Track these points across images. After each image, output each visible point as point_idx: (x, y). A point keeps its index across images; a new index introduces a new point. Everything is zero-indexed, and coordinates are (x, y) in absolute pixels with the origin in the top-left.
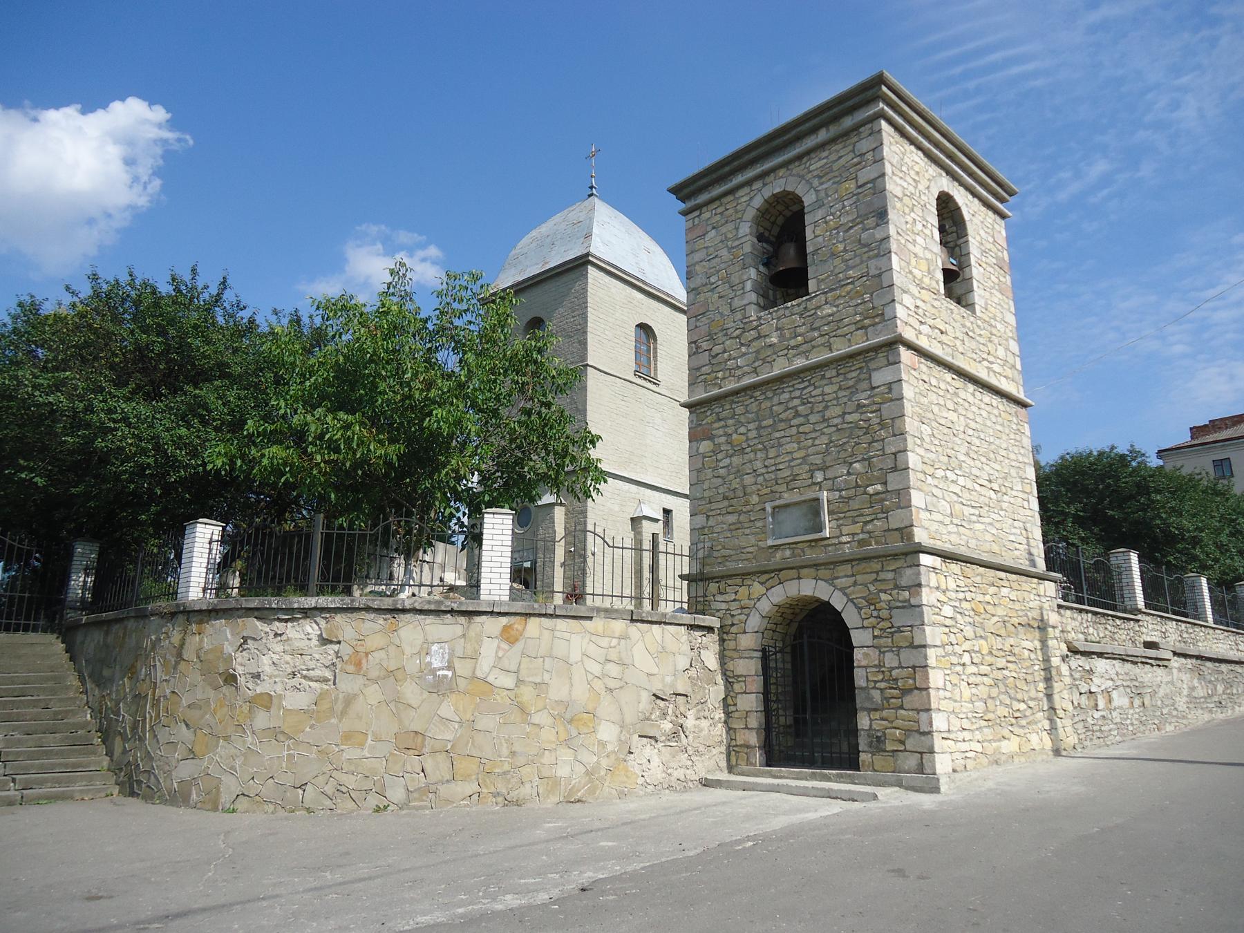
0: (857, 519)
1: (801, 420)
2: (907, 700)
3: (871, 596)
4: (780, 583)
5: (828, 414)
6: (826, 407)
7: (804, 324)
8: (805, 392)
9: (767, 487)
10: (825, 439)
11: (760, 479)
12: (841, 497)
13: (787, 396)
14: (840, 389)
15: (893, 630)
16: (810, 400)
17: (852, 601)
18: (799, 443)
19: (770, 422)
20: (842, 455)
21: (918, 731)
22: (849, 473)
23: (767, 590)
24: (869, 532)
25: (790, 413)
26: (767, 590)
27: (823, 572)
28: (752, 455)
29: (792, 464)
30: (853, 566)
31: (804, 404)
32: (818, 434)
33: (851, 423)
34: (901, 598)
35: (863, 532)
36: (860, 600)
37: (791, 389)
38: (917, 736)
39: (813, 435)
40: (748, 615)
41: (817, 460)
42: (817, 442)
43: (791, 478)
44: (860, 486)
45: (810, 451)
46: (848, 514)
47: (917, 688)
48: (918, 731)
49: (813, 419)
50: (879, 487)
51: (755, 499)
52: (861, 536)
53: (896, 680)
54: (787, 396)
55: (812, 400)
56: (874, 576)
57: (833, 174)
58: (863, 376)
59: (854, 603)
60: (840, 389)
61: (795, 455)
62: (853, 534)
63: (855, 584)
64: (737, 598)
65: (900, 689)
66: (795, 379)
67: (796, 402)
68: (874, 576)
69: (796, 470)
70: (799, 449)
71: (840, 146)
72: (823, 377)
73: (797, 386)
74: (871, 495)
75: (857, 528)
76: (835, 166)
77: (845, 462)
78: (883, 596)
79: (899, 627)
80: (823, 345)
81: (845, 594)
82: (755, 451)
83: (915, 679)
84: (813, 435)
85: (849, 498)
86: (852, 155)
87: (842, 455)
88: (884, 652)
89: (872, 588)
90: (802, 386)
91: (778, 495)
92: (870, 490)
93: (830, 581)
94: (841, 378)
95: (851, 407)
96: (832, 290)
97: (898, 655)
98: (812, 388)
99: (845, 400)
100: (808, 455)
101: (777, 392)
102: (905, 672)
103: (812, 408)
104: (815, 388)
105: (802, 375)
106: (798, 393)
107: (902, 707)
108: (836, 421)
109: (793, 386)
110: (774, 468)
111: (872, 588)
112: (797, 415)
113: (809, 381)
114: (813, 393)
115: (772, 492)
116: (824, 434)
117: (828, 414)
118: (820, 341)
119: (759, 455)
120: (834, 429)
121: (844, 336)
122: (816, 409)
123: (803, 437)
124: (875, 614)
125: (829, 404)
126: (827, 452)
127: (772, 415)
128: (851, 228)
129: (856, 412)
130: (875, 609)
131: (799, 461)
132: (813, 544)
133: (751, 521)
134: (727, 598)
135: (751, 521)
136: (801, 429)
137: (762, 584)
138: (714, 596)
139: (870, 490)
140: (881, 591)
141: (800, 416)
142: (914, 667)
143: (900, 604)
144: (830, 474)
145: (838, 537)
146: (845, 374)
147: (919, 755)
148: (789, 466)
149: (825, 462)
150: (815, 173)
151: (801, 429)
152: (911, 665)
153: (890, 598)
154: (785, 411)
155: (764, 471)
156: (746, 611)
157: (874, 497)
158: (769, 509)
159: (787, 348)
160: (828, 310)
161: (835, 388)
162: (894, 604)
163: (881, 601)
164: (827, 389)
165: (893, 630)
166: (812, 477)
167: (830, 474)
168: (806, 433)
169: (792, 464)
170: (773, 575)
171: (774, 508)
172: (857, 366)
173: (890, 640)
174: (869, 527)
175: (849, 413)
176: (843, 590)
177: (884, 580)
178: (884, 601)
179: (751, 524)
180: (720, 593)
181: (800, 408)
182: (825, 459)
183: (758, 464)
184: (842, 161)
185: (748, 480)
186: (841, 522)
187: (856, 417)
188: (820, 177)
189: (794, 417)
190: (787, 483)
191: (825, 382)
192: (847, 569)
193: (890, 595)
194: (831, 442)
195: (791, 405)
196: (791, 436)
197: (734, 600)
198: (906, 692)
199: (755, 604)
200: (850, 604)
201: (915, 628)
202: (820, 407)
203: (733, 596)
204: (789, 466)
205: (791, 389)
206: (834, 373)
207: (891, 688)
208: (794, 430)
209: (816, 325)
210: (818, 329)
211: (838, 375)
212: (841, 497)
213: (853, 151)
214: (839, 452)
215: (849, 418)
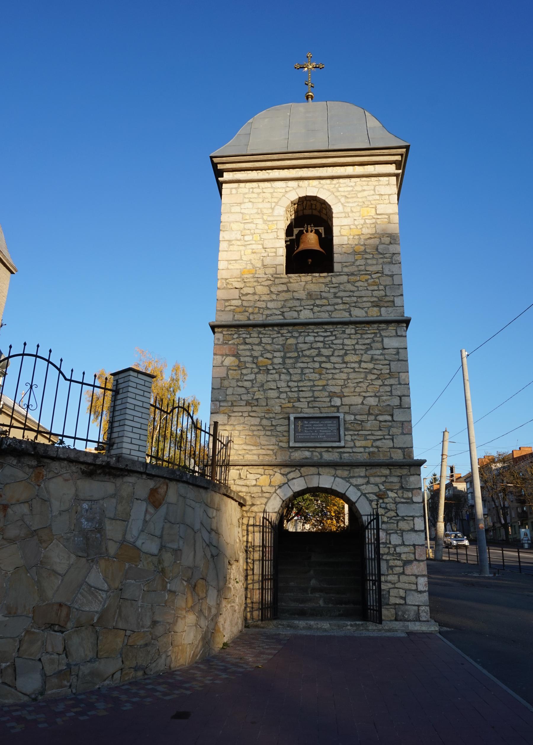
0: (368, 437)
1: (324, 359)
2: (409, 570)
3: (381, 493)
4: (301, 476)
5: (347, 359)
6: (346, 354)
7: (329, 292)
8: (327, 339)
9: (289, 402)
10: (344, 376)
11: (283, 396)
12: (355, 419)
13: (311, 339)
14: (357, 343)
15: (398, 518)
16: (331, 346)
17: (364, 495)
18: (320, 374)
19: (296, 354)
20: (358, 390)
21: (416, 591)
22: (362, 403)
23: (288, 480)
24: (377, 447)
25: (314, 352)
26: (288, 480)
27: (339, 472)
28: (277, 376)
29: (314, 389)
30: (366, 470)
31: (324, 348)
32: (338, 371)
33: (366, 369)
34: (405, 496)
35: (372, 446)
36: (371, 495)
37: (316, 335)
38: (416, 594)
39: (333, 371)
40: (269, 499)
41: (337, 389)
42: (336, 376)
43: (313, 399)
44: (372, 414)
45: (330, 382)
46: (361, 432)
47: (416, 560)
48: (416, 591)
49: (333, 359)
50: (389, 418)
51: (278, 409)
52: (371, 449)
53: (400, 554)
54: (311, 339)
55: (333, 346)
56: (383, 479)
57: (355, 200)
58: (376, 339)
59: (367, 498)
60: (357, 343)
61: (316, 383)
62: (365, 447)
63: (368, 483)
64: (258, 484)
65: (402, 560)
66: (319, 328)
67: (321, 345)
68: (383, 479)
69: (316, 394)
70: (320, 379)
71: (364, 183)
72: (344, 332)
73: (320, 334)
74: (380, 421)
75: (369, 443)
76: (360, 195)
77: (359, 395)
78: (391, 494)
79: (403, 517)
80: (344, 310)
81: (359, 490)
82: (280, 374)
83: (414, 553)
84: (333, 371)
85: (362, 421)
86: (372, 192)
87: (358, 390)
88: (390, 534)
89: (382, 487)
90: (325, 334)
91: (300, 410)
92: (381, 418)
93: (346, 479)
94: (359, 336)
95: (366, 357)
96: (352, 274)
97: (402, 536)
98: (334, 338)
99: (362, 352)
100: (327, 385)
101: (302, 334)
102: (406, 549)
103: (333, 352)
104: (336, 339)
105: (326, 327)
106: (321, 339)
107: (403, 573)
108: (353, 365)
109: (317, 333)
110: (296, 389)
111: (382, 487)
112: (319, 355)
113: (331, 332)
114: (335, 342)
115: (293, 406)
116: (342, 372)
117: (347, 359)
118: (341, 307)
119: (283, 377)
120: (352, 370)
121: (362, 308)
122: (336, 353)
123: (324, 371)
124: (383, 505)
125: (348, 352)
126: (344, 386)
127: (296, 350)
128: (371, 238)
129: (370, 362)
130: (383, 502)
131: (321, 388)
132: (330, 450)
133: (272, 425)
134: (248, 483)
135: (272, 425)
136: (323, 365)
137: (283, 475)
138: (234, 480)
139: (381, 418)
140: (388, 490)
141: (322, 355)
142: (414, 545)
143: (404, 501)
144: (346, 401)
145: (352, 448)
146: (361, 334)
147: (416, 608)
148: (310, 390)
149: (343, 392)
150: (343, 194)
151: (323, 365)
152: (412, 543)
153: (396, 495)
154: (309, 349)
155: (288, 389)
156: (267, 495)
157: (383, 423)
158: (292, 418)
159: (313, 305)
160: (349, 287)
161: (354, 342)
162: (398, 500)
163: (388, 497)
164: (347, 342)
165: (398, 518)
166: (330, 401)
167: (346, 401)
168: (327, 369)
169: (314, 389)
170: (294, 469)
171: (295, 418)
172: (372, 331)
173: (395, 525)
174: (378, 443)
175: (365, 362)
176: (357, 486)
177: (392, 482)
178: (391, 497)
179: (273, 428)
180: (241, 478)
181: (322, 350)
182: (343, 390)
183: (284, 384)
184: (365, 194)
185: (273, 394)
186: (355, 437)
187: (371, 366)
188: (346, 197)
189: (317, 355)
190: (308, 402)
191: (345, 336)
192: (362, 471)
193: (396, 493)
194: (349, 379)
195: (315, 345)
196: (314, 369)
197: (255, 485)
198: (407, 563)
199: (276, 490)
200: (363, 497)
201: (416, 519)
202: (342, 352)
203: (254, 483)
204: (310, 390)
205: (316, 335)
206: (353, 331)
207: (394, 559)
208: (317, 365)
209: (340, 294)
210: (342, 298)
211: (356, 333)
212: (355, 419)
213: (374, 190)
214: (355, 388)
215: (363, 365)
